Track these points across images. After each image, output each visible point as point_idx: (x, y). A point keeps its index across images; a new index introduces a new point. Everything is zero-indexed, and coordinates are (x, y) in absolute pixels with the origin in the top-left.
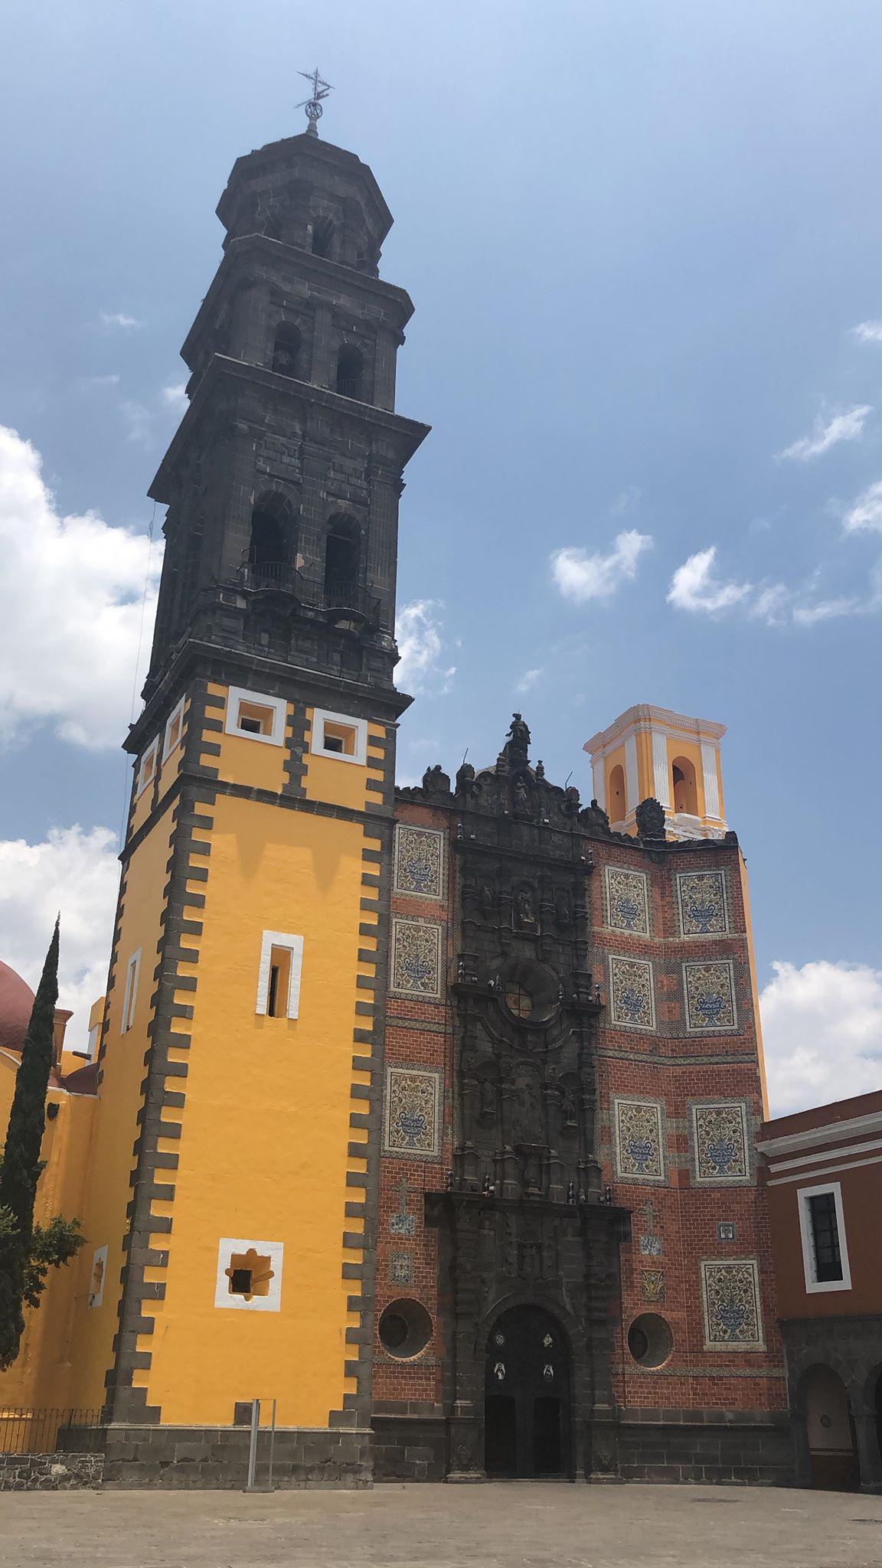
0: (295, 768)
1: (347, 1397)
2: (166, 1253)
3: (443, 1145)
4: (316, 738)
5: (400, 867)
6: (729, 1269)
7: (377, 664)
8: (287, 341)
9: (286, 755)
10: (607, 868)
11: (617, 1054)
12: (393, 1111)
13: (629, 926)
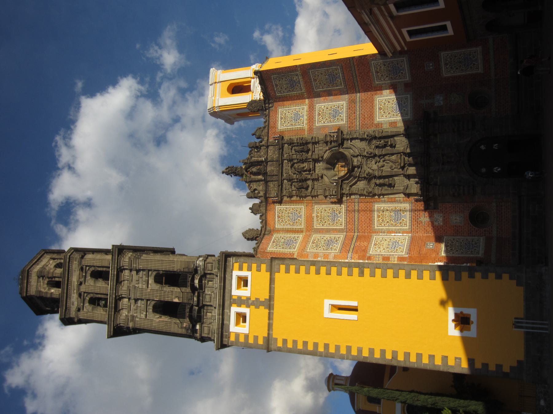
0: (257, 303)
1: (511, 278)
2: (456, 358)
4: (245, 293)
5: (293, 225)
6: (446, 64)
9: (253, 307)
10: (279, 128)
11: (358, 121)
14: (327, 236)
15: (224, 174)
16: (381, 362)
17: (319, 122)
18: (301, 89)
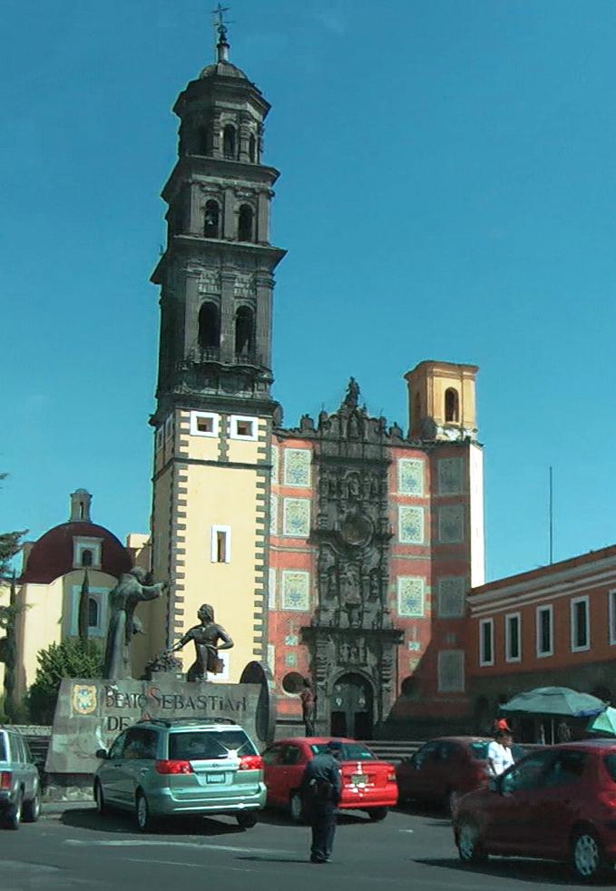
0: (223, 447)
7: (262, 386)
8: (212, 209)
12: (286, 591)
13: (411, 490)
15: (350, 381)
17: (404, 510)
18: (443, 492)
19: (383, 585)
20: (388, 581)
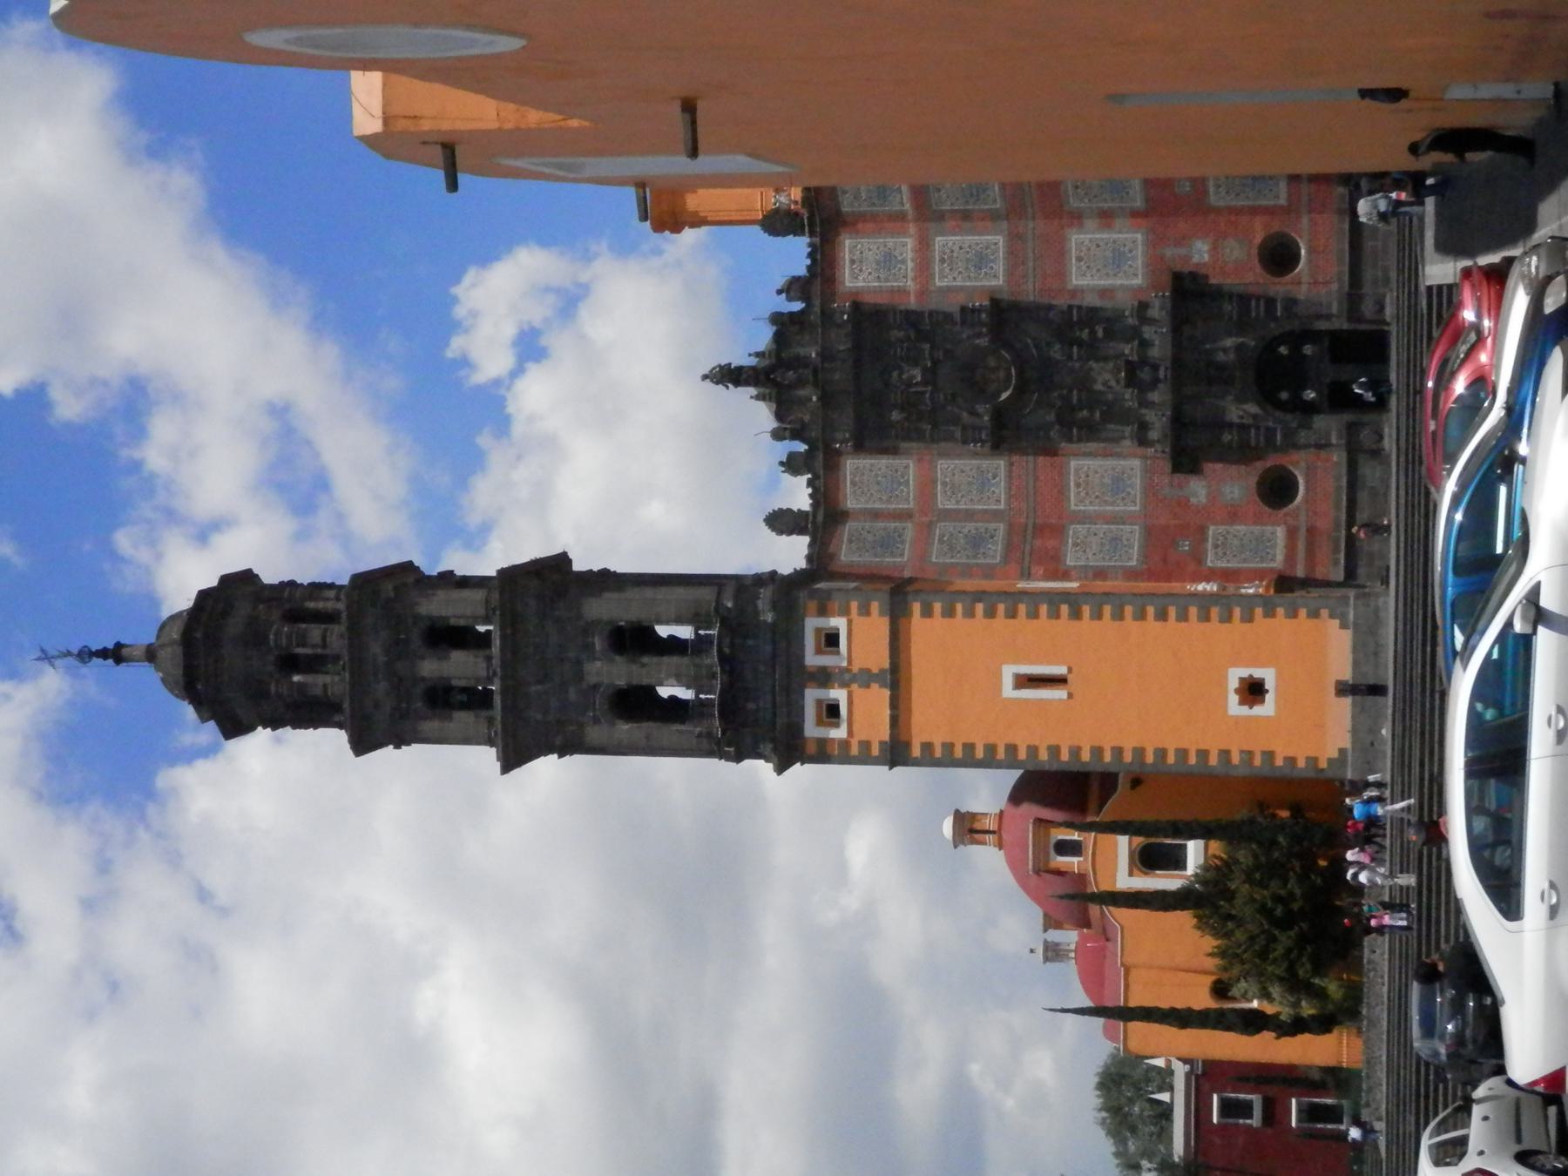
1: (1332, 616)
2: (1242, 752)
3: (1135, 456)
5: (889, 501)
13: (904, 262)
14: (970, 527)
15: (708, 383)
16: (1113, 769)
17: (942, 277)
19: (1091, 316)
20: (1080, 307)
